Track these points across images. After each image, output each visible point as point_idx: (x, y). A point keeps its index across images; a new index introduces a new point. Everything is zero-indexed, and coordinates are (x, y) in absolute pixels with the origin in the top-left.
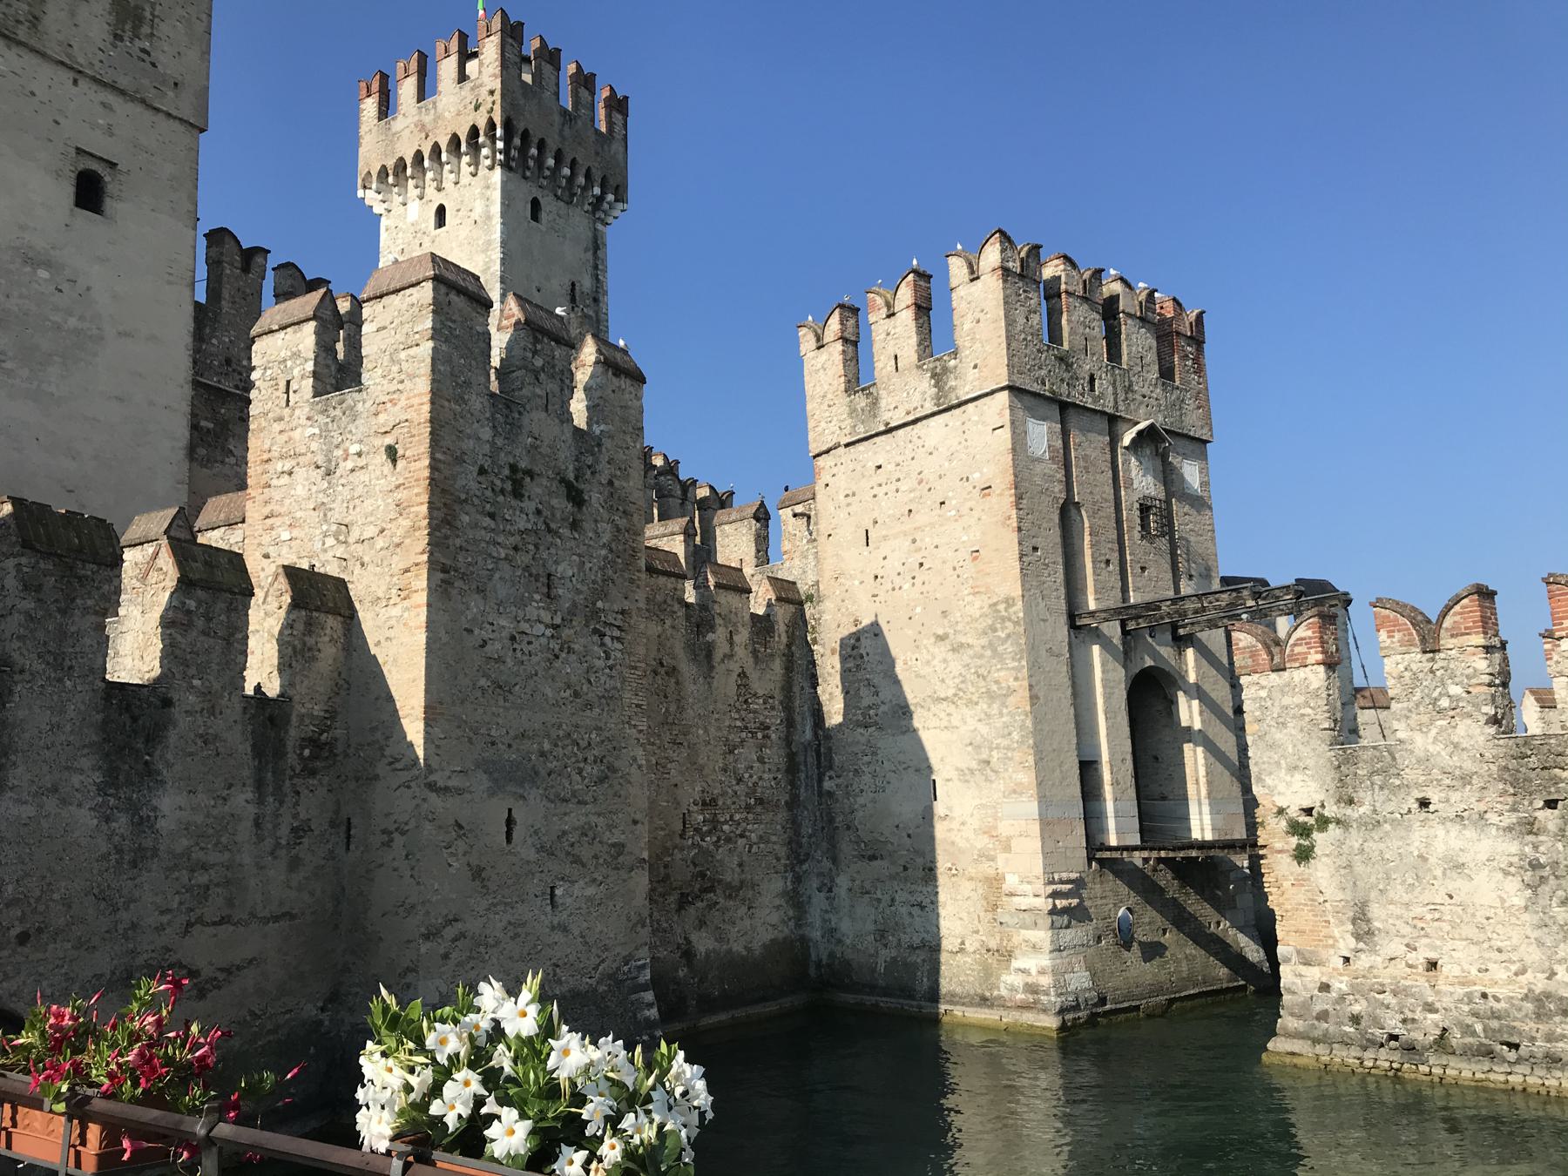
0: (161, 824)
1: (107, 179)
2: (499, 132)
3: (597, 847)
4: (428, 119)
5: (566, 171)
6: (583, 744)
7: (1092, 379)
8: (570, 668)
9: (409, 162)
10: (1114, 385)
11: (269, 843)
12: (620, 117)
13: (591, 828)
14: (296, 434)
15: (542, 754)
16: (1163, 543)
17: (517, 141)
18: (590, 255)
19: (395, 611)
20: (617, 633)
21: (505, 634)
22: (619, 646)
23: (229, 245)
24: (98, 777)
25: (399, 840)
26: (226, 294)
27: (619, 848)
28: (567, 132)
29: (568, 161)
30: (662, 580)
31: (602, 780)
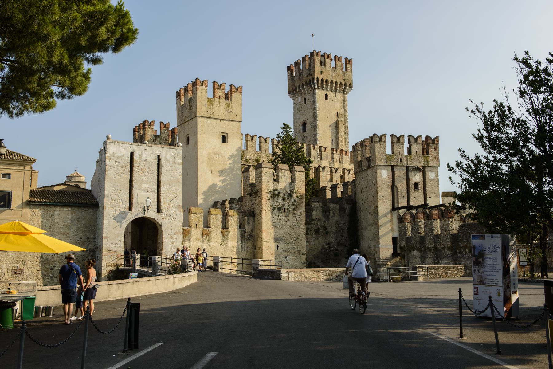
0: (229, 246)
1: (226, 136)
2: (315, 81)
3: (295, 251)
4: (301, 77)
5: (334, 85)
6: (292, 235)
7: (401, 159)
8: (289, 223)
9: (297, 88)
10: (407, 159)
11: (243, 249)
12: (350, 65)
13: (293, 247)
14: (248, 189)
15: (284, 236)
16: (421, 192)
17: (320, 82)
18: (342, 104)
19: (259, 217)
20: (299, 216)
21: (276, 219)
22: (299, 218)
23: (249, 136)
24: (221, 240)
25: (260, 249)
26: (249, 147)
27: (300, 251)
28: (334, 75)
29: (334, 82)
30: (316, 203)
31: (295, 240)
